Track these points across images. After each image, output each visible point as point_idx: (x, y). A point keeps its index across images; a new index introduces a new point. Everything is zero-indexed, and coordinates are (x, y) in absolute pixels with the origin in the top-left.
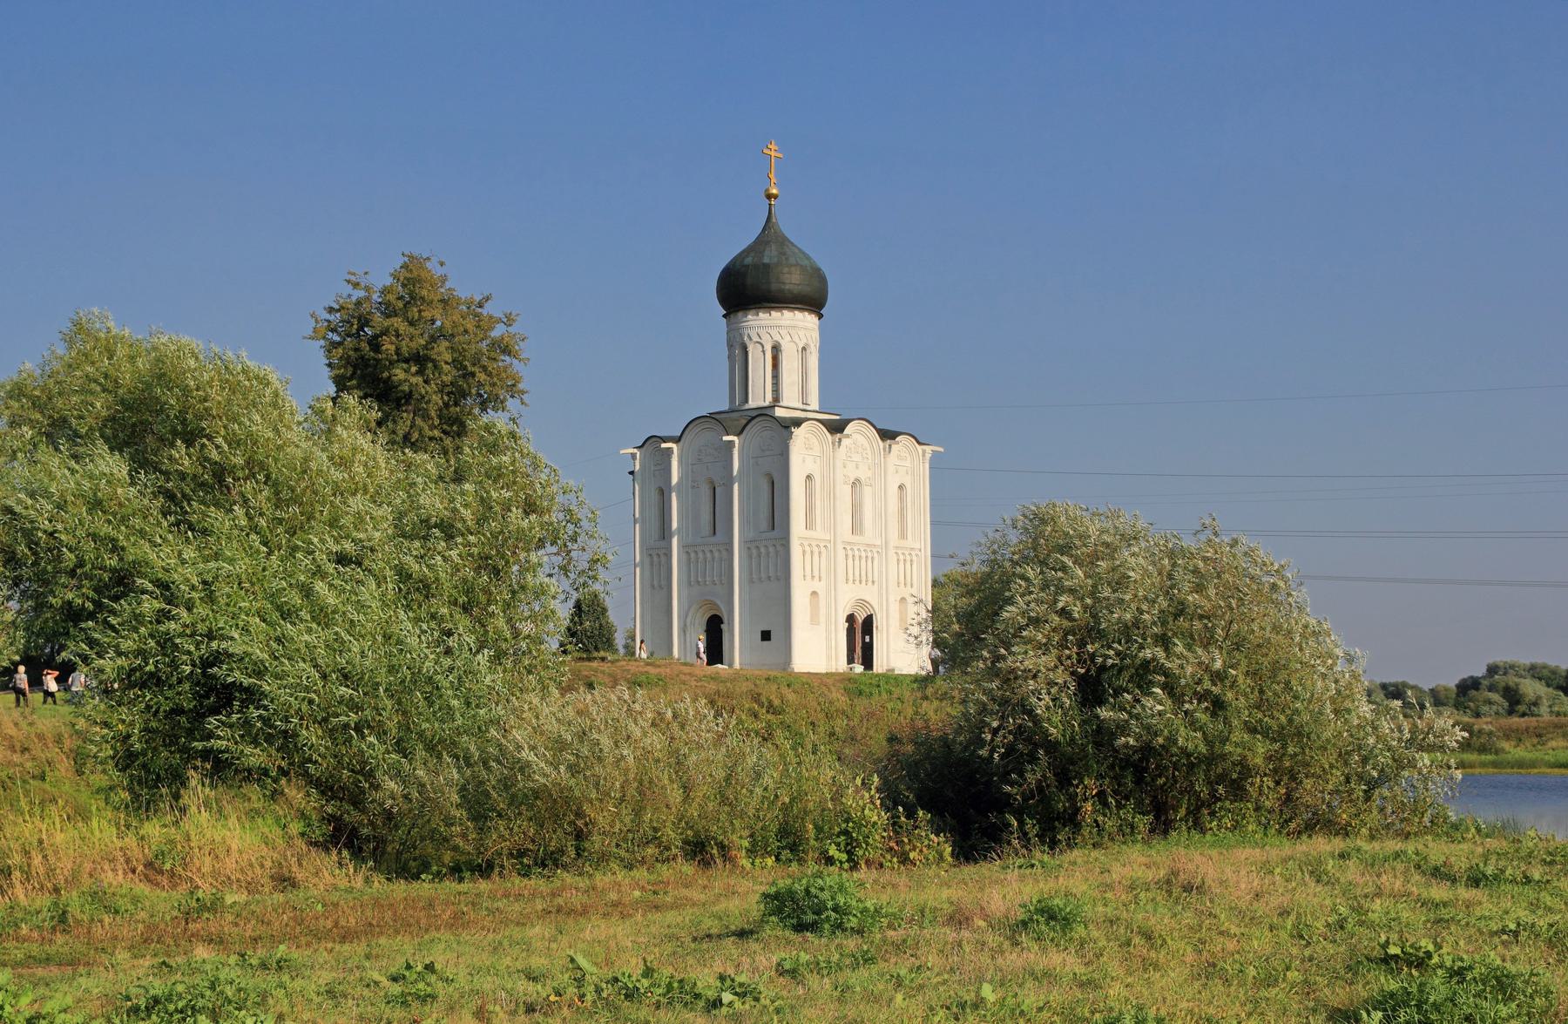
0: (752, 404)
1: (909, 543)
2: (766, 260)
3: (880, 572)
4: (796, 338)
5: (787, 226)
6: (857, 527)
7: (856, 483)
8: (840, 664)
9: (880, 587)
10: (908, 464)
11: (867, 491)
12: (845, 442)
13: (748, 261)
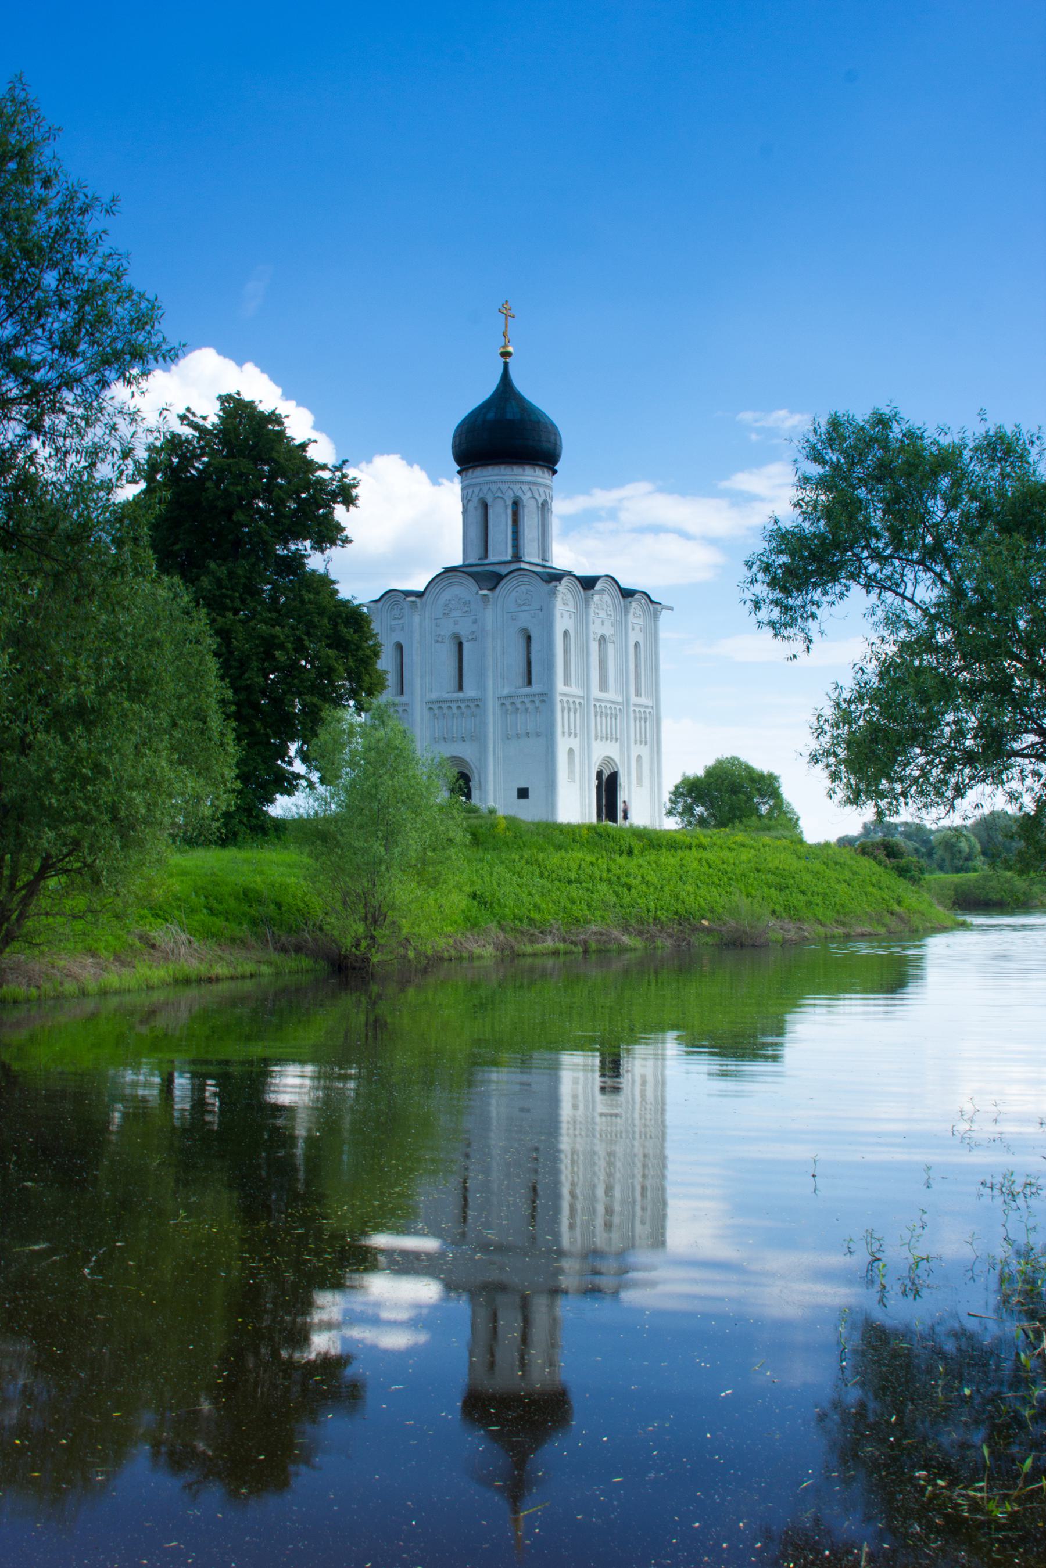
0: (492, 559)
1: (643, 700)
2: (509, 416)
3: (622, 730)
4: (536, 496)
5: (522, 385)
6: (603, 686)
7: (603, 637)
8: (594, 820)
9: (622, 745)
10: (641, 621)
11: (611, 648)
12: (596, 597)
13: (491, 416)
